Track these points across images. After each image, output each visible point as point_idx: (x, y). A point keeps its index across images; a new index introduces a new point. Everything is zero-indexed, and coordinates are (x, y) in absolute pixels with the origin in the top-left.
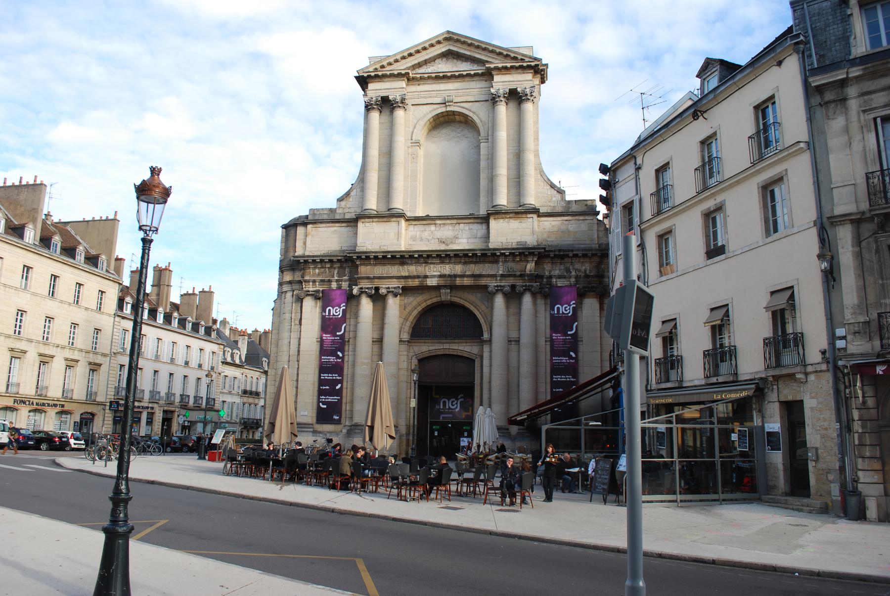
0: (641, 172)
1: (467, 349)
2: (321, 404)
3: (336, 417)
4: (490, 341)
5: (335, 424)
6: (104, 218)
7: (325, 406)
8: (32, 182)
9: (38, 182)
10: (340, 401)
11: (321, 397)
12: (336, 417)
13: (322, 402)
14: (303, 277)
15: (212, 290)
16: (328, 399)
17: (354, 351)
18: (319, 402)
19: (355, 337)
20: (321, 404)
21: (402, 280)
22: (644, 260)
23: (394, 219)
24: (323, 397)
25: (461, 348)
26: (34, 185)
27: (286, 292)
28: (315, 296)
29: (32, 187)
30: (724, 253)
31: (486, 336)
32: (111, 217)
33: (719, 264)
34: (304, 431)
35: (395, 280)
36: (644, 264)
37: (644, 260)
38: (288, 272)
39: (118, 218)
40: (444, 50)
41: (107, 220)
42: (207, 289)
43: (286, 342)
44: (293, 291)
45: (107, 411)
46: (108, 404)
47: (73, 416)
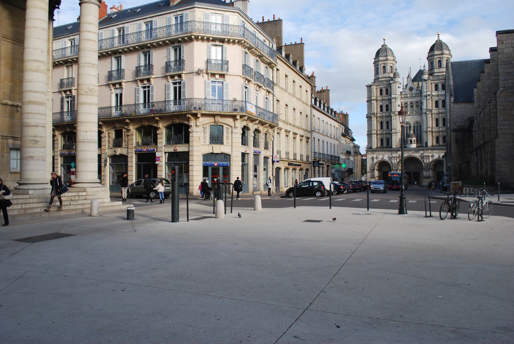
6: (294, 43)
8: (271, 19)
9: (276, 19)
15: (328, 89)
26: (274, 21)
29: (273, 23)
32: (299, 42)
39: (303, 42)
41: (296, 44)
42: (325, 88)
45: (312, 167)
46: (312, 163)
47: (303, 171)
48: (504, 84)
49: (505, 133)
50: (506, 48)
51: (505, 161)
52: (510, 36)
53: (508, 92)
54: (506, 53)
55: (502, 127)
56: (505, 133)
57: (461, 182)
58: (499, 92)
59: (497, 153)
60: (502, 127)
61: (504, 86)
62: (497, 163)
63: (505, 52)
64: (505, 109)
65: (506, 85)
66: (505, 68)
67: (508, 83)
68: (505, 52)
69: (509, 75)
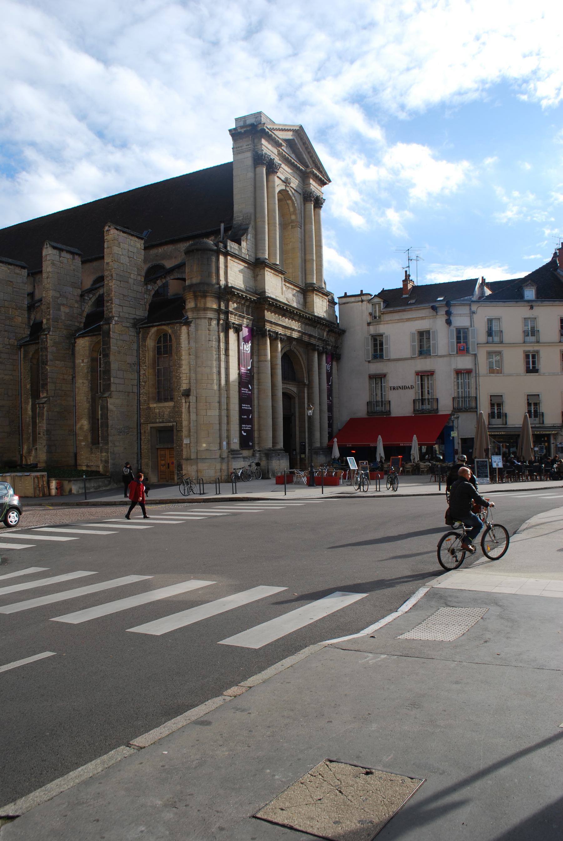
0: (475, 316)
1: (293, 389)
2: (243, 432)
3: (251, 444)
4: (310, 386)
5: (249, 449)
7: (245, 434)
10: (252, 428)
11: (243, 426)
12: (251, 444)
13: (243, 430)
14: (227, 306)
16: (247, 427)
17: (259, 383)
18: (241, 430)
19: (258, 373)
20: (243, 432)
21: (284, 329)
22: (475, 362)
23: (280, 275)
24: (244, 426)
25: (290, 388)
27: (211, 319)
28: (238, 330)
30: (537, 372)
31: (306, 381)
33: (532, 377)
34: (238, 457)
35: (281, 328)
36: (475, 364)
37: (475, 362)
38: (213, 299)
40: (291, 137)
43: (215, 370)
44: (219, 320)
48: (119, 312)
49: (119, 391)
50: (122, 255)
51: (119, 435)
52: (127, 238)
53: (123, 325)
54: (123, 264)
55: (117, 381)
56: (119, 391)
57: (46, 473)
58: (114, 322)
59: (110, 422)
60: (117, 381)
61: (119, 315)
62: (110, 438)
63: (121, 262)
64: (119, 352)
65: (121, 314)
66: (121, 287)
67: (123, 312)
68: (121, 262)
69: (125, 298)
